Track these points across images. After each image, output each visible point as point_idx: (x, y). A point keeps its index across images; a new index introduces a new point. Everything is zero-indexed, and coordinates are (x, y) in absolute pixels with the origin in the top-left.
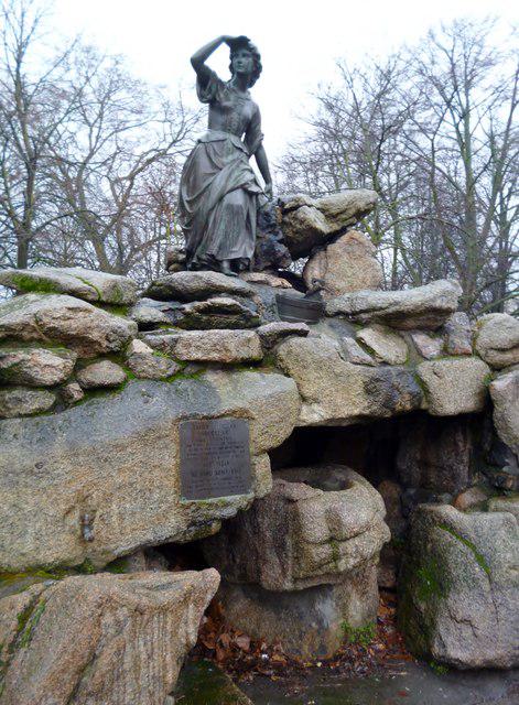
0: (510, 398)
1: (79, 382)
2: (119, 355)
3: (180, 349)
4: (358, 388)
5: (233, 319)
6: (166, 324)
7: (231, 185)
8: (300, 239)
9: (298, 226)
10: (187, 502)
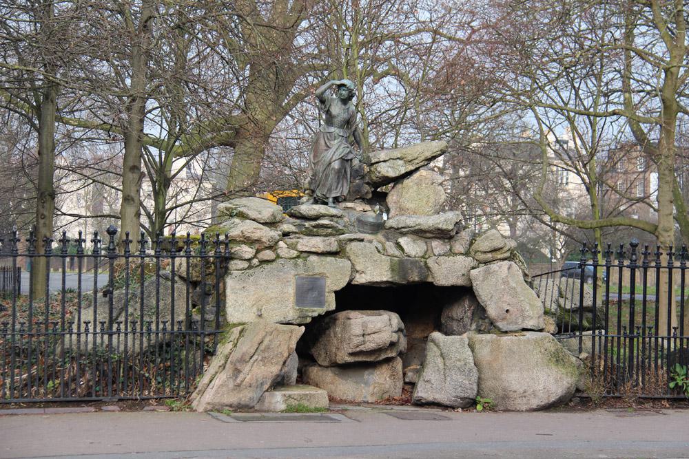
0: (481, 279)
2: (273, 247)
5: (330, 231)
6: (295, 233)
7: (334, 159)
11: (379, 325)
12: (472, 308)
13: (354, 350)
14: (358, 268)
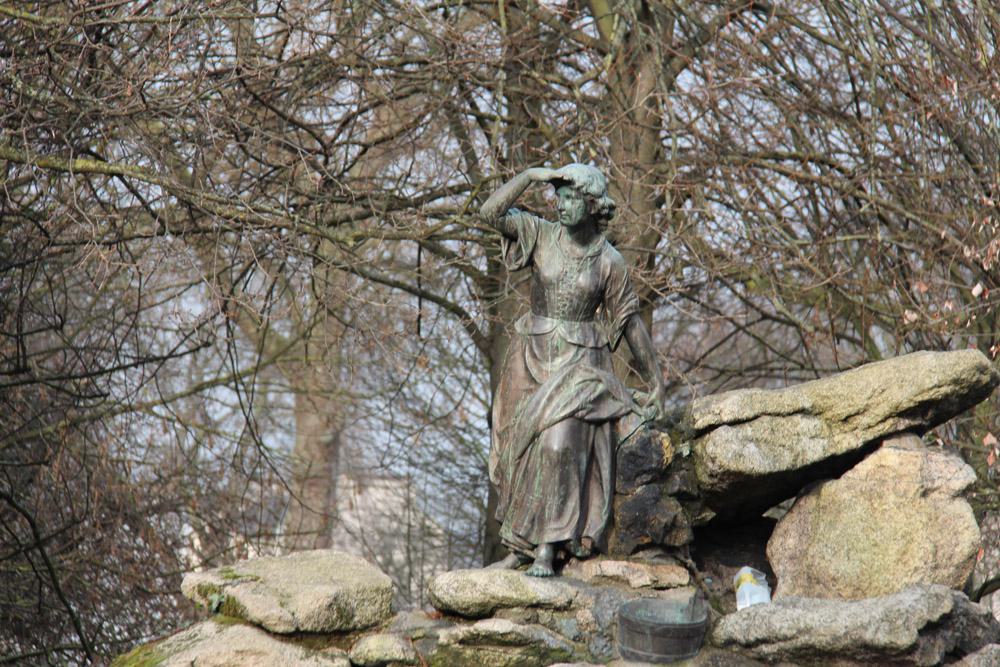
9: (710, 465)
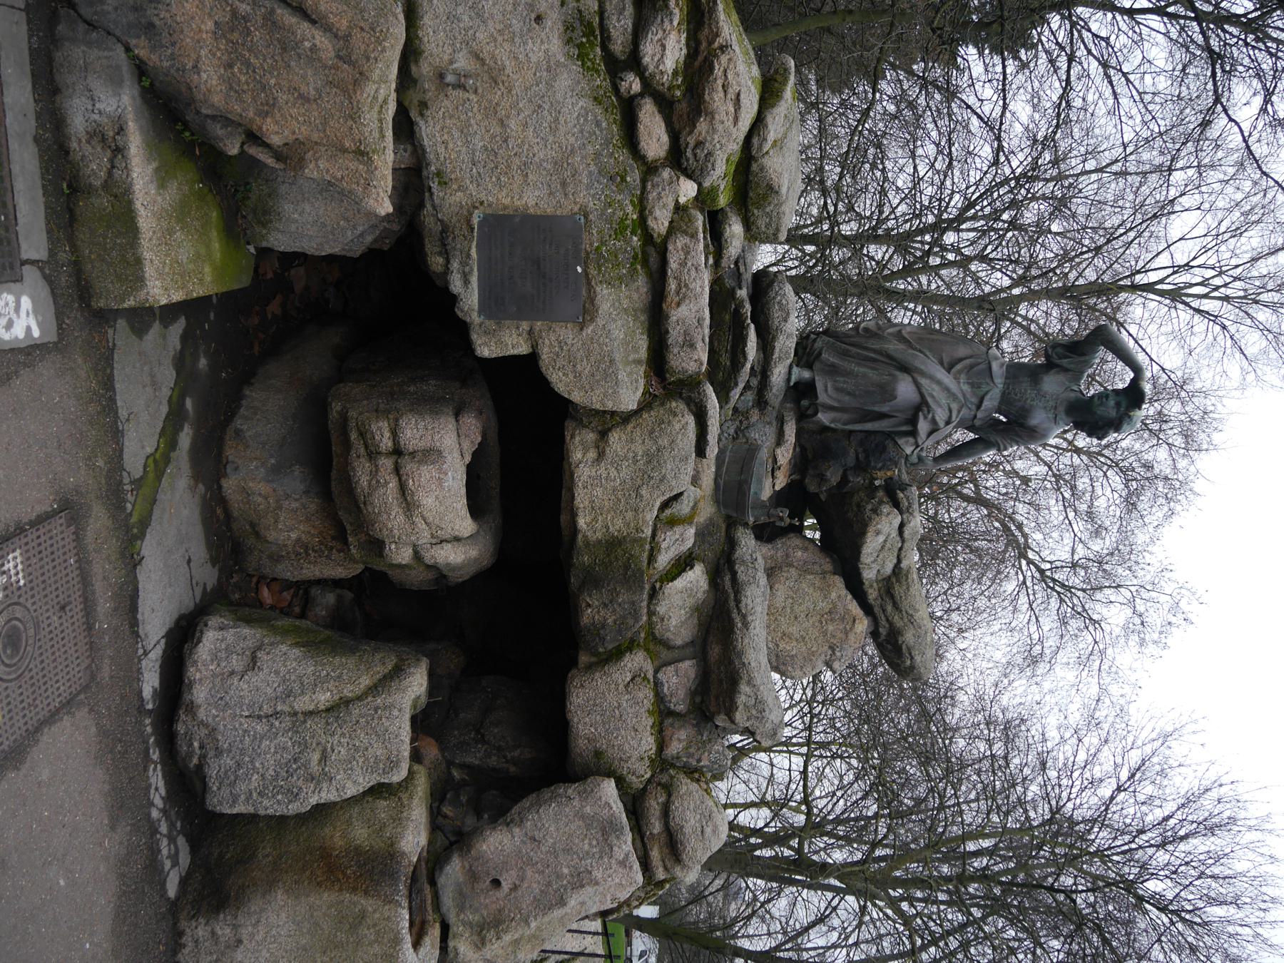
0: (588, 809)
1: (642, 95)
2: (677, 159)
3: (681, 241)
4: (617, 526)
5: (725, 360)
7: (923, 381)
8: (850, 515)
9: (869, 507)
10: (475, 221)
11: (428, 501)
12: (512, 769)
13: (352, 424)
14: (615, 437)
